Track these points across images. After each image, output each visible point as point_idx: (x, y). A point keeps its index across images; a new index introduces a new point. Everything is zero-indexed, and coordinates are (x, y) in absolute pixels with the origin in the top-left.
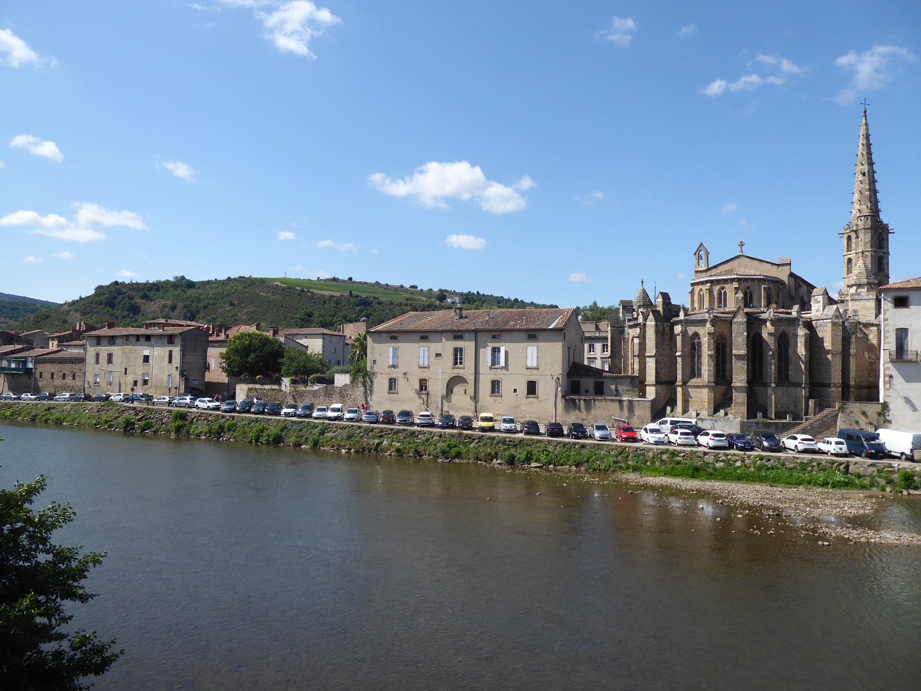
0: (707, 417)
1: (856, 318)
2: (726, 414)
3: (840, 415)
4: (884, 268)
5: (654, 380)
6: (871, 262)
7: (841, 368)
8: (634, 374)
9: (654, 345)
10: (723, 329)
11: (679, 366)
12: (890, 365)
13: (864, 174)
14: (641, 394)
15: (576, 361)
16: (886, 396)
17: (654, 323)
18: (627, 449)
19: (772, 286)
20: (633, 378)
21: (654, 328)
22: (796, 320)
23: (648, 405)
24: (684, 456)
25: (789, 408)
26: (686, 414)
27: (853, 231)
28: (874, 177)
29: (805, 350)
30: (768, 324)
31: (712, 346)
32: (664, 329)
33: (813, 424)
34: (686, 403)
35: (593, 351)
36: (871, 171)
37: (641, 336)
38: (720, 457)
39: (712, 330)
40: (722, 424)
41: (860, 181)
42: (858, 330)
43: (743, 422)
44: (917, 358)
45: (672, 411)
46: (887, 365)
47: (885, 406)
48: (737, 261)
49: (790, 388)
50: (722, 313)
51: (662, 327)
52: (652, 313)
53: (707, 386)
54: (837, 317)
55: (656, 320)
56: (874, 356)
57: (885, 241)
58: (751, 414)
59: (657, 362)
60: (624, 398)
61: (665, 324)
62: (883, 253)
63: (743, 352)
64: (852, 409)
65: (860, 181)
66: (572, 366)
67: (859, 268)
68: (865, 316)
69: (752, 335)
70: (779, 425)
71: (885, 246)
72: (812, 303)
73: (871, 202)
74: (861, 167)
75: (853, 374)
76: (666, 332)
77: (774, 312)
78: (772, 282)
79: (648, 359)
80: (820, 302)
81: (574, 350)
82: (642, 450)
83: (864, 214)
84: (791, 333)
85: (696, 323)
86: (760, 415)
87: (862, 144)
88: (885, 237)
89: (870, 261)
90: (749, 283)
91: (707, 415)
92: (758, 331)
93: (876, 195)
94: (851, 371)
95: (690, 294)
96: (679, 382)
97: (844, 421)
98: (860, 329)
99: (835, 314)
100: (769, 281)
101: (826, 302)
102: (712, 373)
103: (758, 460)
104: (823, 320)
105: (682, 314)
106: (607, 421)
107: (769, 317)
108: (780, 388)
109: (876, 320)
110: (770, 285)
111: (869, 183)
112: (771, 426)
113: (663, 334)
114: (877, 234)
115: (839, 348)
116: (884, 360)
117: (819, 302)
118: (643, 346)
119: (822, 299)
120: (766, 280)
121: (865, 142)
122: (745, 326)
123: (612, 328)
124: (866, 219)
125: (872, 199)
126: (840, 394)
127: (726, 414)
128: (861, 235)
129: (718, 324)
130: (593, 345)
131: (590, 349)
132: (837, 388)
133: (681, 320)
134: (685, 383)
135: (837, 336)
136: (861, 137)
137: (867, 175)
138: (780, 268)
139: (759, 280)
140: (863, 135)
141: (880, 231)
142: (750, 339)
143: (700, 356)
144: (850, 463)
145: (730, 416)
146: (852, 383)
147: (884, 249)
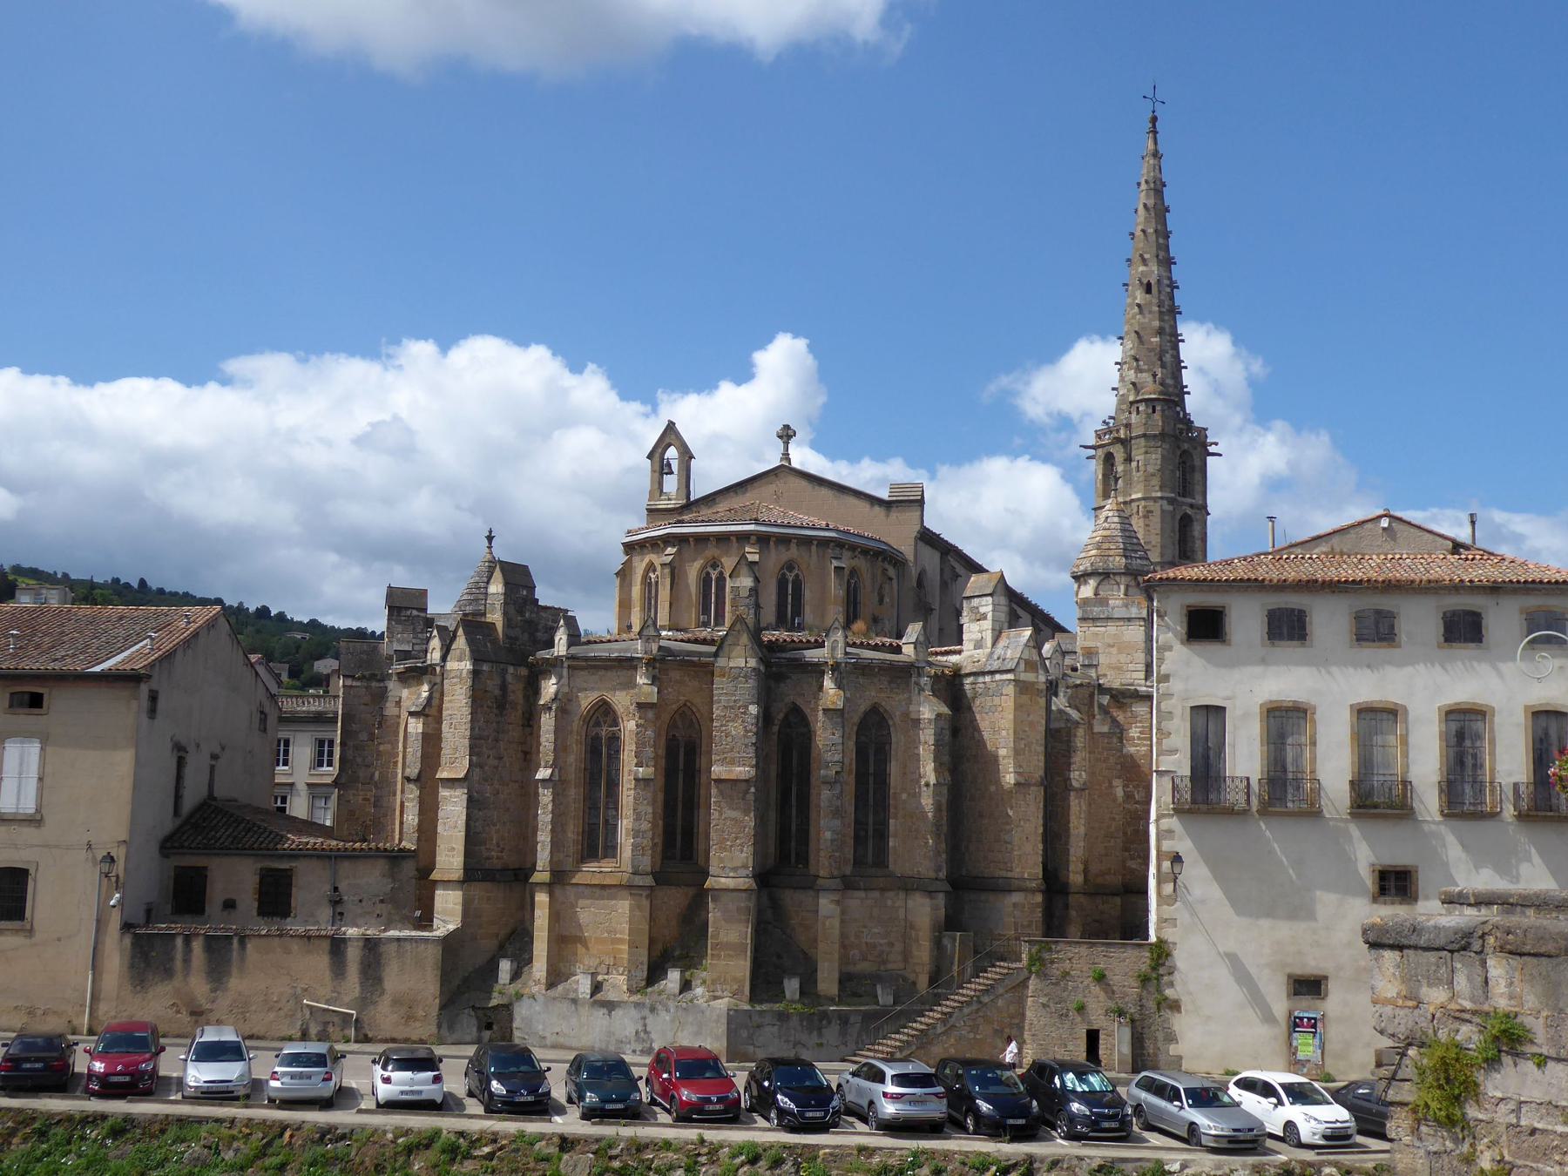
0: (625, 997)
1: (1093, 673)
2: (686, 986)
3: (1033, 983)
5: (461, 865)
7: (1041, 830)
8: (404, 844)
9: (466, 742)
10: (685, 690)
11: (544, 817)
12: (1173, 823)
14: (418, 913)
15: (220, 792)
16: (1166, 920)
17: (467, 665)
18: (287, 1134)
19: (862, 563)
20: (397, 857)
21: (469, 683)
22: (914, 672)
23: (432, 955)
24: (490, 1156)
25: (884, 962)
26: (560, 988)
27: (1118, 440)
28: (1172, 298)
29: (936, 770)
30: (828, 683)
31: (649, 751)
32: (504, 687)
33: (950, 1014)
34: (565, 941)
35: (286, 763)
36: (1166, 282)
37: (433, 711)
38: (615, 1157)
39: (651, 694)
40: (672, 1021)
41: (1139, 306)
42: (1096, 709)
43: (736, 1011)
44: (1248, 801)
45: (516, 975)
46: (1167, 823)
47: (1161, 953)
48: (769, 489)
49: (891, 894)
50: (689, 641)
51: (498, 681)
52: (466, 633)
53: (629, 887)
54: (1030, 666)
55: (476, 660)
56: (1143, 794)
57: (1197, 476)
58: (764, 982)
59: (472, 803)
60: (352, 932)
61: (511, 669)
62: (1192, 506)
63: (743, 771)
64: (1067, 965)
65: (1139, 306)
66: (186, 822)
67: (1107, 525)
68: (1118, 668)
69: (781, 716)
70: (852, 1020)
71: (1198, 488)
72: (964, 620)
73: (1163, 366)
74: (1142, 268)
75: (1077, 849)
76: (511, 697)
77: (848, 644)
78: (865, 552)
79: (444, 793)
80: (985, 618)
81: (214, 757)
82: (343, 1137)
83: (1147, 397)
84: (897, 713)
85: (606, 668)
86: (792, 986)
87: (1145, 205)
88: (1197, 462)
90: (794, 552)
91: (625, 987)
92: (800, 702)
93: (1176, 349)
94: (1072, 840)
95: (617, 581)
96: (542, 876)
97: (1044, 1006)
98: (1101, 706)
99: (1026, 656)
100: (853, 548)
101: (1003, 617)
102: (647, 842)
103: (742, 1165)
104: (992, 673)
105: (561, 638)
106: (286, 1016)
107: (833, 657)
108: (862, 894)
109: (1148, 684)
110: (855, 562)
111: (1161, 313)
112: (824, 1022)
113: (502, 704)
114: (1179, 453)
115: (1036, 765)
116: (1159, 807)
117: (984, 617)
118: (432, 741)
119: (990, 608)
120: (840, 544)
121: (1151, 202)
122: (752, 683)
123: (349, 682)
124: (1150, 411)
125: (1168, 358)
126: (1039, 914)
127: (686, 986)
128: (1138, 455)
129: (675, 675)
130: (287, 743)
131: (321, 754)
132: (1030, 896)
133: (557, 658)
134: (559, 877)
135: (1031, 724)
136: (1144, 186)
137: (1154, 289)
138: (894, 515)
139: (824, 543)
140: (1147, 182)
141: (1186, 446)
142: (776, 729)
143: (613, 785)
144: (1036, 1165)
145: (699, 991)
146: (1076, 878)
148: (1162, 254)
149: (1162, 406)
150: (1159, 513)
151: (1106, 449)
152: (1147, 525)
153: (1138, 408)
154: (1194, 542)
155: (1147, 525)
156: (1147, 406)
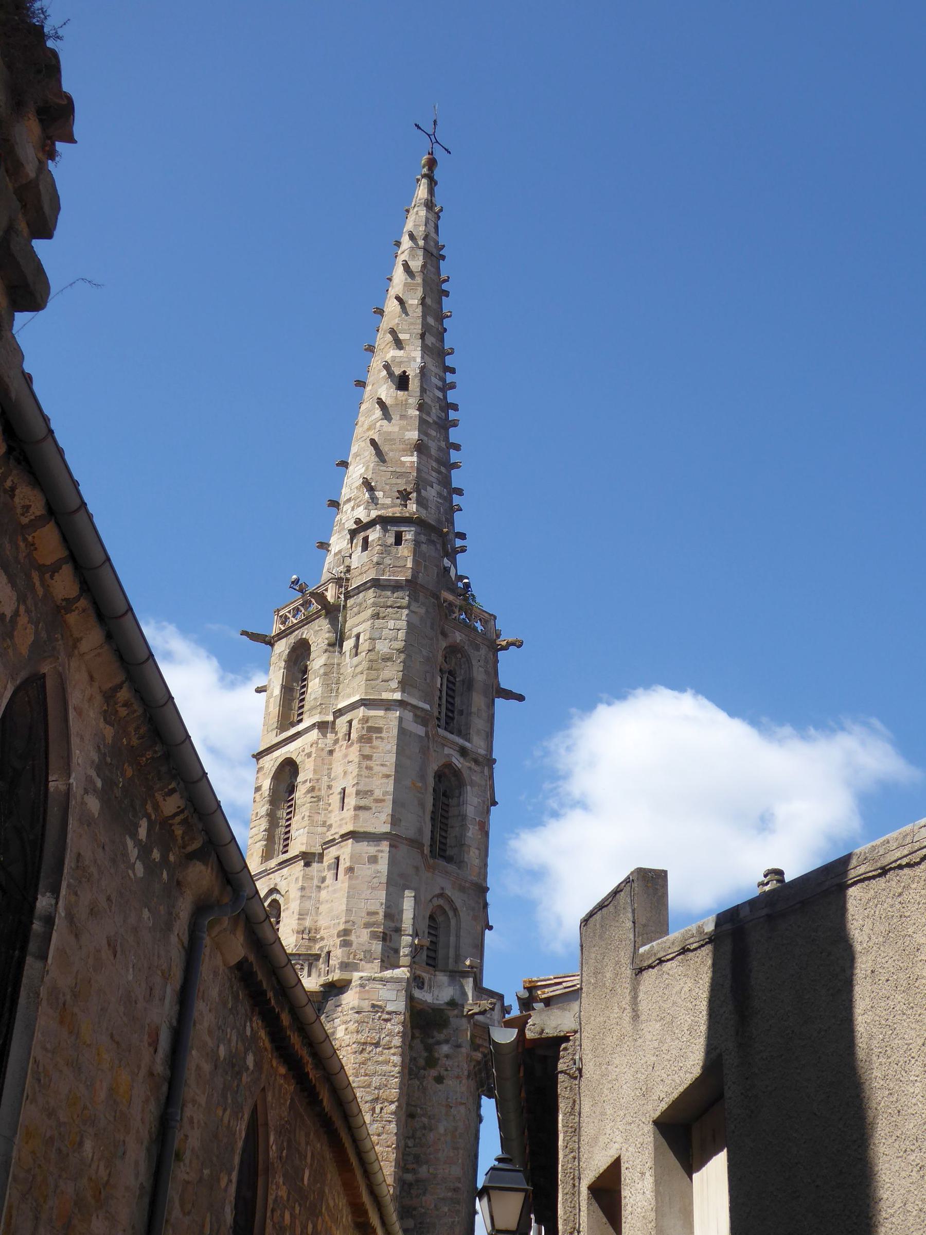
4: (461, 844)
6: (399, 766)
13: (402, 382)
62: (463, 752)
89: (391, 759)
124: (391, 540)
137: (414, 384)
140: (412, 237)
141: (458, 637)
147: (468, 740)
148: (430, 340)
149: (417, 534)
150: (395, 732)
151: (292, 639)
152: (368, 757)
153: (366, 540)
154: (464, 827)
155: (368, 757)
156: (385, 530)
